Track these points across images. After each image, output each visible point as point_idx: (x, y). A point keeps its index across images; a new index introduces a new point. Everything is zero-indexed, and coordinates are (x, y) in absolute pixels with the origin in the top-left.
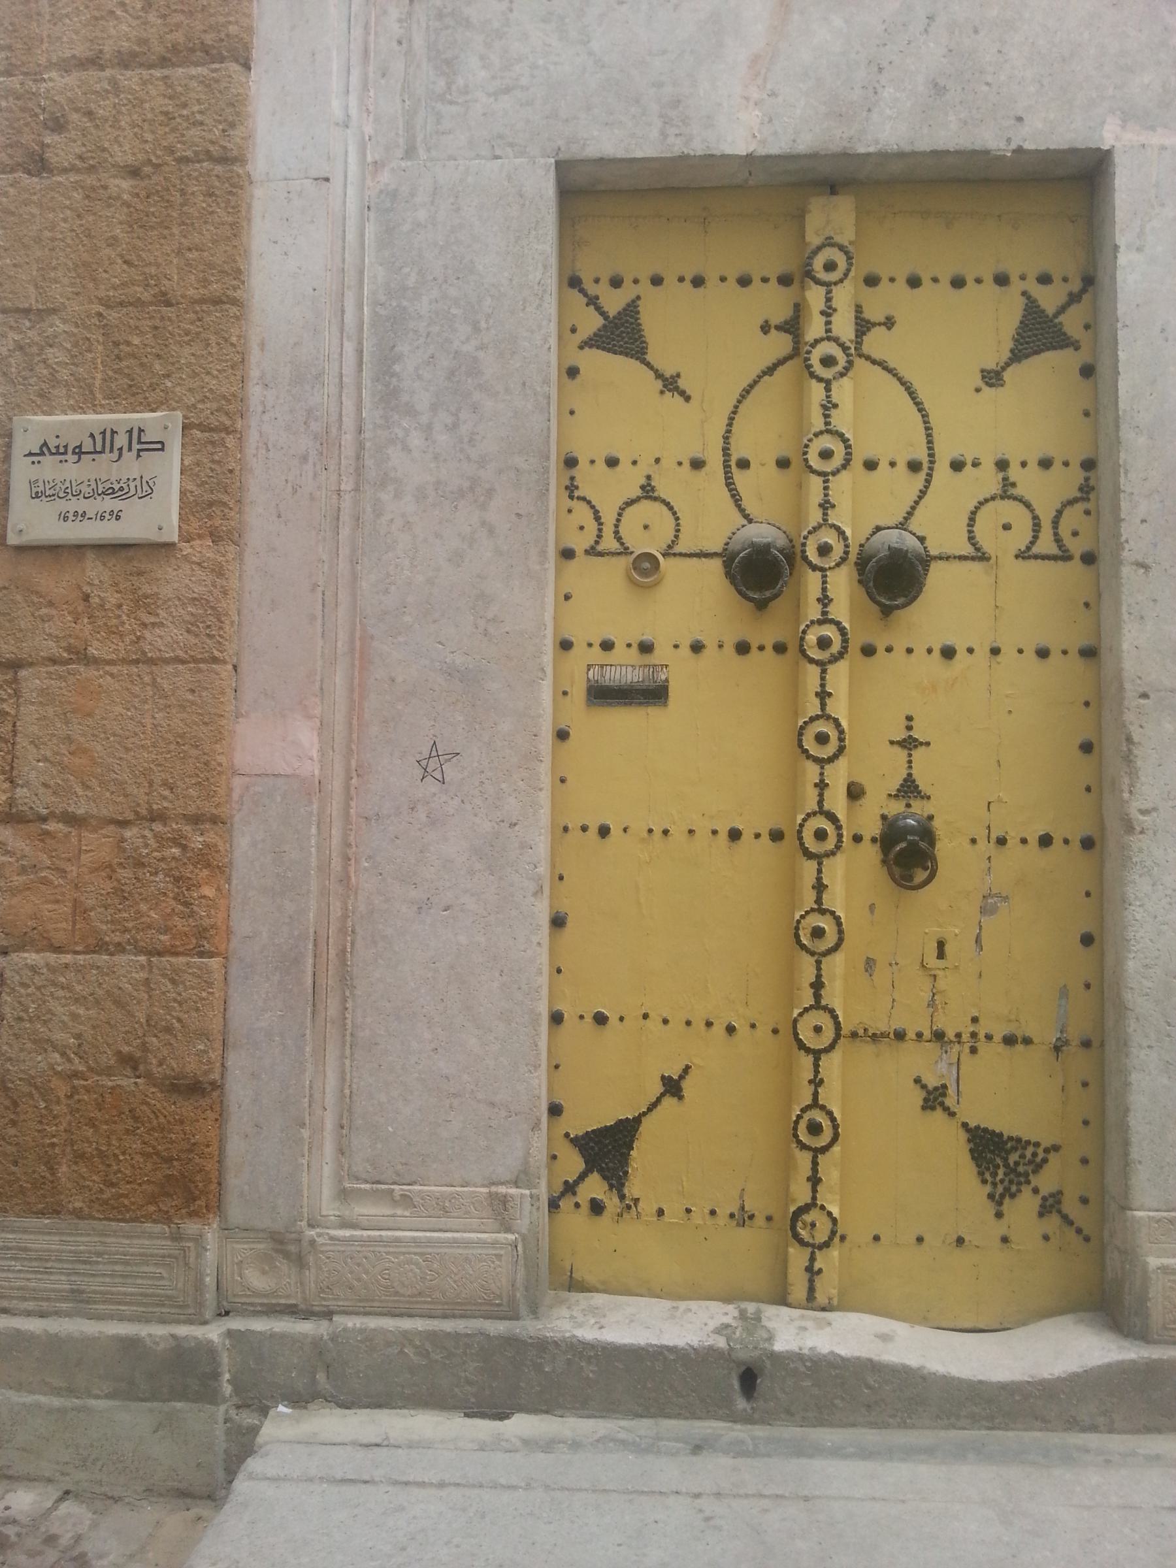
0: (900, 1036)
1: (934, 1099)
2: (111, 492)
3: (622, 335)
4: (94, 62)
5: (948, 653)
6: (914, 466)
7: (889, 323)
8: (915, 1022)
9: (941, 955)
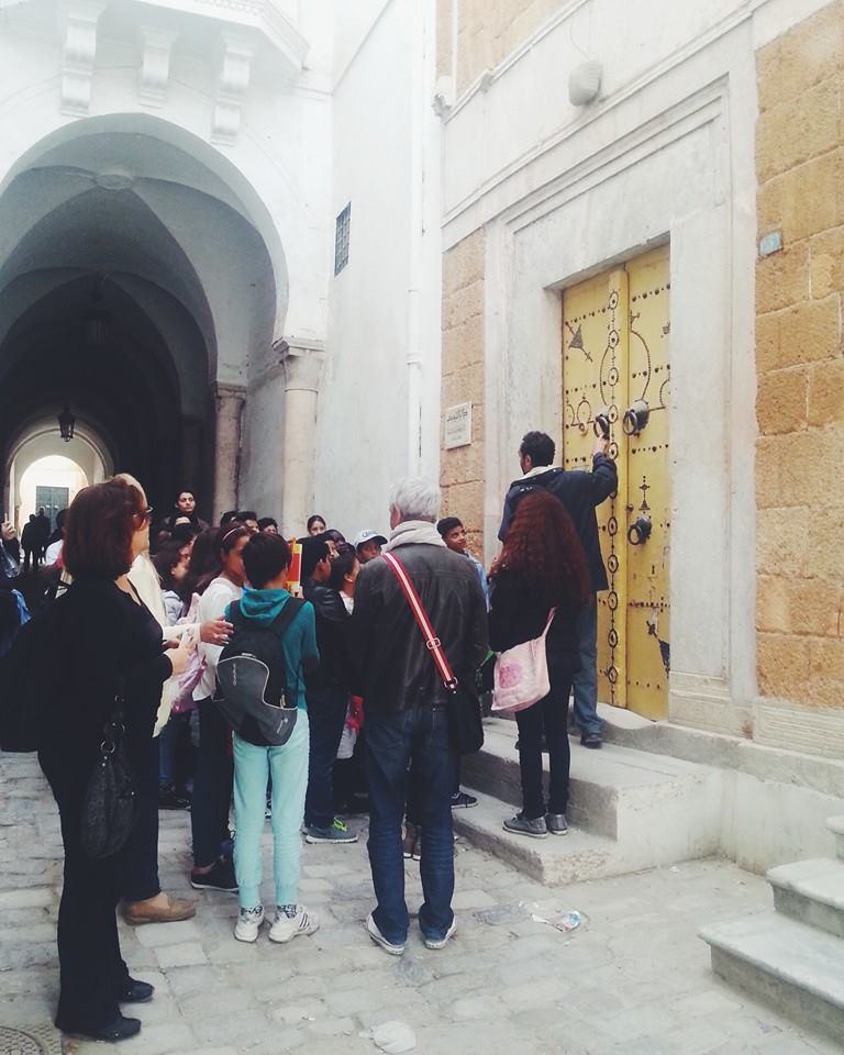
0: (642, 604)
1: (652, 630)
2: (459, 430)
3: (577, 342)
4: (457, 289)
5: (654, 449)
6: (645, 374)
7: (638, 317)
8: (646, 600)
9: (653, 572)
